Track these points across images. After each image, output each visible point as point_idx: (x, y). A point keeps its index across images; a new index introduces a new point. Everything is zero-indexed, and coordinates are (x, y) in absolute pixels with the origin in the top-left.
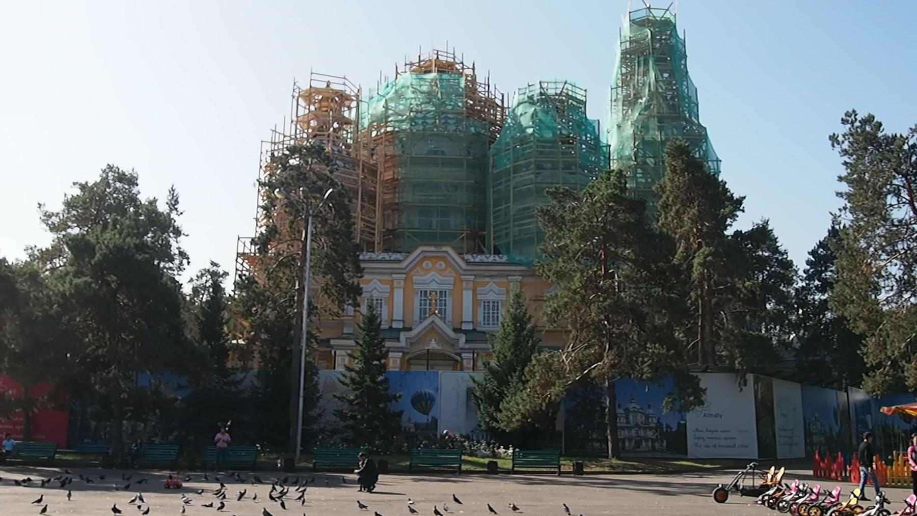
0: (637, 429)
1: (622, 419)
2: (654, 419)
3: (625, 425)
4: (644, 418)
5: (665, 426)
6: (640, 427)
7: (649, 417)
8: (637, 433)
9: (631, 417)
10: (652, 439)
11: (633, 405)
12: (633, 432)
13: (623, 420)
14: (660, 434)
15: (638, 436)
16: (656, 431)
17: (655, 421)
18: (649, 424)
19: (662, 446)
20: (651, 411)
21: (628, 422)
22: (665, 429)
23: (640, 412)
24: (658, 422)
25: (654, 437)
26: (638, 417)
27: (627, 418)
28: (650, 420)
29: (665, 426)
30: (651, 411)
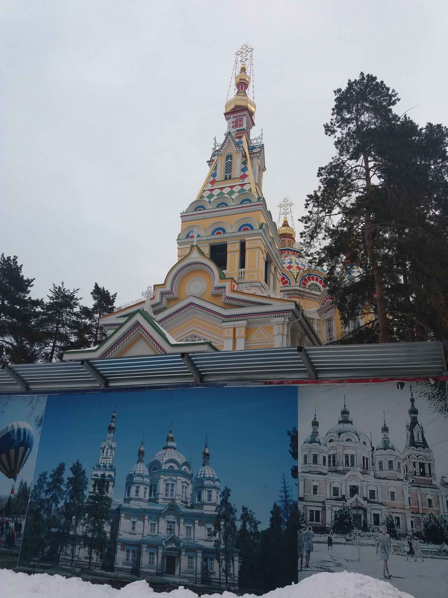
0: (171, 518)
1: (142, 489)
2: (214, 493)
3: (145, 505)
4: (189, 490)
5: (238, 515)
6: (179, 515)
7: (204, 487)
8: (170, 529)
9: (161, 487)
10: (205, 551)
11: (170, 454)
12: (163, 524)
13: (144, 492)
14: (225, 538)
15: (173, 540)
16: (217, 526)
17: (216, 498)
18: (201, 506)
19: (226, 571)
20: (209, 472)
21: (154, 500)
22: (239, 525)
23: (184, 474)
24: (225, 502)
25: (210, 545)
26: (178, 488)
27: (153, 488)
28: (205, 495)
29: (238, 515)
30: (209, 472)
